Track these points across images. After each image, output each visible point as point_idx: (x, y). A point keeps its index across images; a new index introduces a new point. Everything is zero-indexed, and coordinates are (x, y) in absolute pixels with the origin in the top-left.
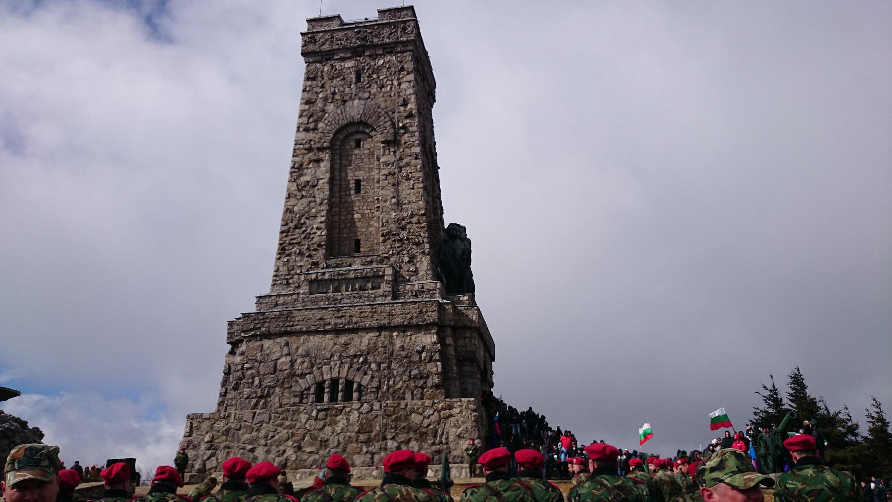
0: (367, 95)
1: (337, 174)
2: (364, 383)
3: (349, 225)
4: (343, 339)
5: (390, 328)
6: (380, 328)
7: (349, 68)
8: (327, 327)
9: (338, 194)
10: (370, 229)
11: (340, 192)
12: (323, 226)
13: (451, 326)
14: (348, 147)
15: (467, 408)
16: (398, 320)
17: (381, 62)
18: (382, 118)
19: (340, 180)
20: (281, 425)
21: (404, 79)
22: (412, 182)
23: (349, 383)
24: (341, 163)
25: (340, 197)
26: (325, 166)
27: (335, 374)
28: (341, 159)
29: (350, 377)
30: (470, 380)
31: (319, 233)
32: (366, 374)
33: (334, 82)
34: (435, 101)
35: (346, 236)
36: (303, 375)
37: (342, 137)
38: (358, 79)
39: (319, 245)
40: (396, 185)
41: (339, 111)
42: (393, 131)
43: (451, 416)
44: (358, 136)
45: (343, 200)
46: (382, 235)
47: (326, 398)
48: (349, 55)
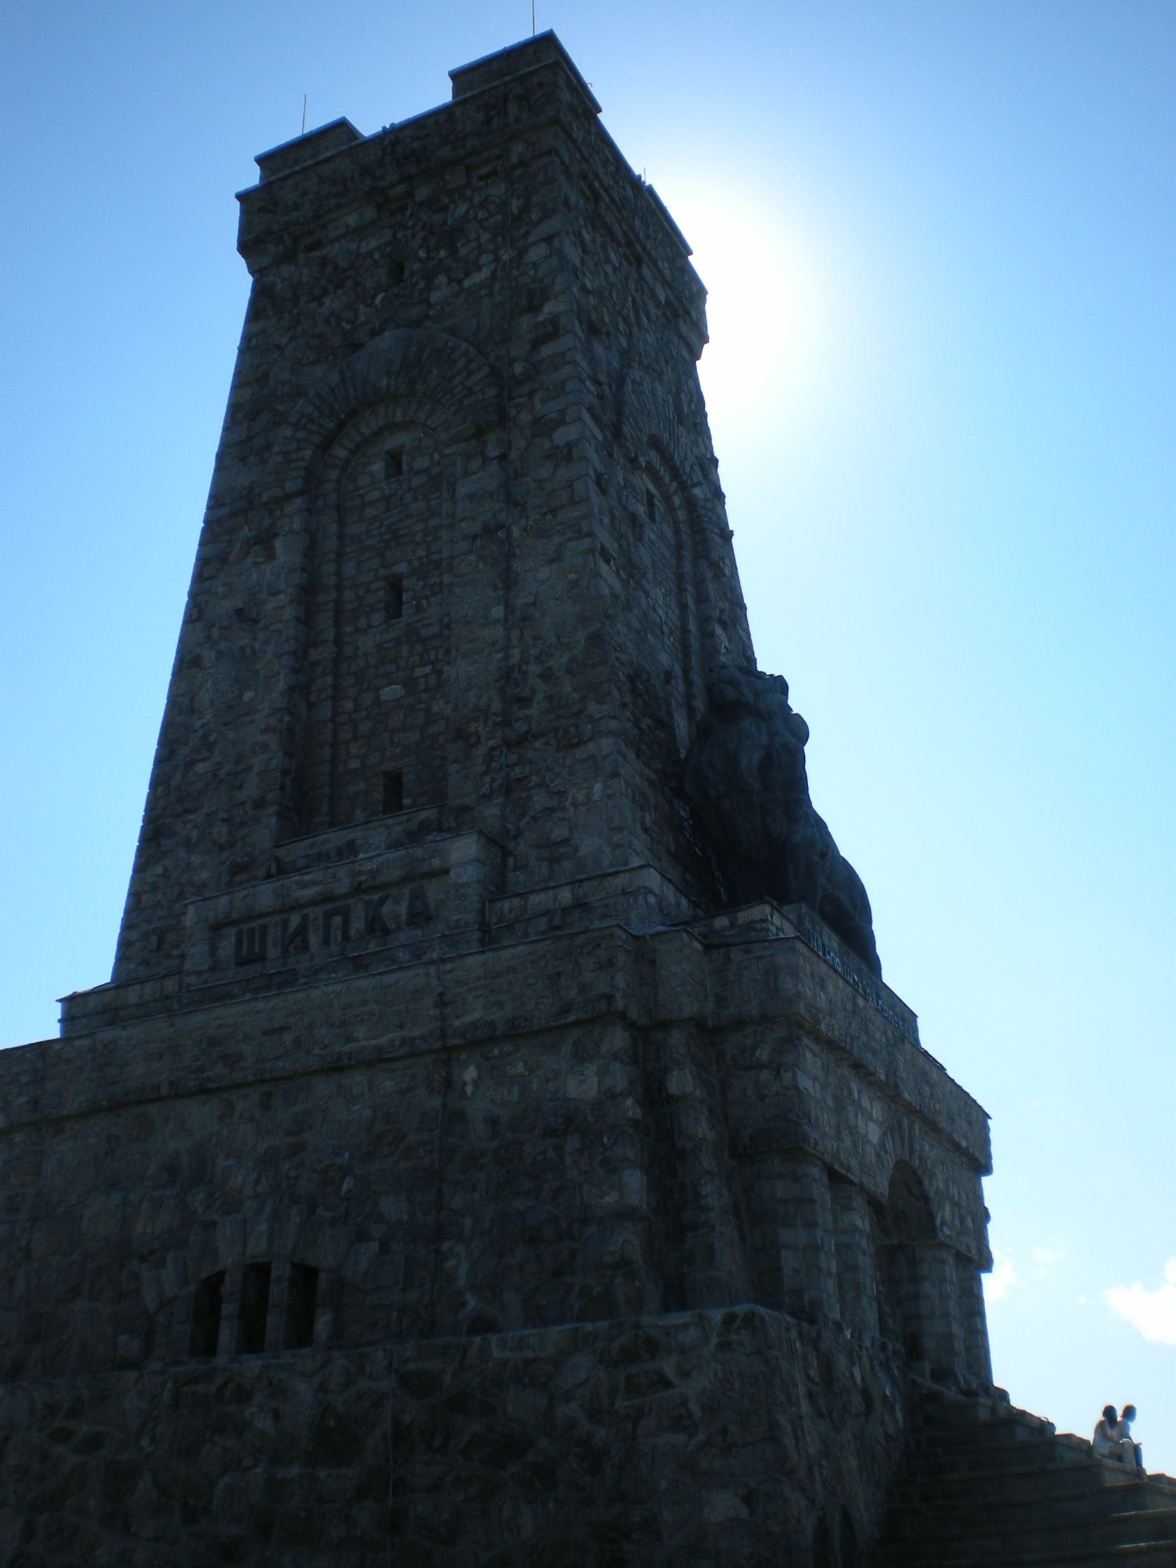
0: (416, 311)
1: (329, 568)
3: (365, 727)
7: (370, 253)
9: (330, 635)
10: (433, 729)
11: (337, 624)
12: (273, 740)
14: (364, 480)
17: (462, 208)
18: (461, 364)
19: (339, 588)
20: (64, 1436)
21: (532, 238)
22: (556, 539)
23: (305, 1275)
24: (341, 536)
25: (338, 641)
27: (257, 1247)
28: (341, 523)
32: (361, 1236)
33: (327, 301)
34: (704, 339)
35: (355, 764)
37: (342, 453)
38: (397, 271)
39: (259, 804)
41: (334, 378)
42: (491, 392)
44: (393, 442)
45: (348, 651)
47: (227, 1335)
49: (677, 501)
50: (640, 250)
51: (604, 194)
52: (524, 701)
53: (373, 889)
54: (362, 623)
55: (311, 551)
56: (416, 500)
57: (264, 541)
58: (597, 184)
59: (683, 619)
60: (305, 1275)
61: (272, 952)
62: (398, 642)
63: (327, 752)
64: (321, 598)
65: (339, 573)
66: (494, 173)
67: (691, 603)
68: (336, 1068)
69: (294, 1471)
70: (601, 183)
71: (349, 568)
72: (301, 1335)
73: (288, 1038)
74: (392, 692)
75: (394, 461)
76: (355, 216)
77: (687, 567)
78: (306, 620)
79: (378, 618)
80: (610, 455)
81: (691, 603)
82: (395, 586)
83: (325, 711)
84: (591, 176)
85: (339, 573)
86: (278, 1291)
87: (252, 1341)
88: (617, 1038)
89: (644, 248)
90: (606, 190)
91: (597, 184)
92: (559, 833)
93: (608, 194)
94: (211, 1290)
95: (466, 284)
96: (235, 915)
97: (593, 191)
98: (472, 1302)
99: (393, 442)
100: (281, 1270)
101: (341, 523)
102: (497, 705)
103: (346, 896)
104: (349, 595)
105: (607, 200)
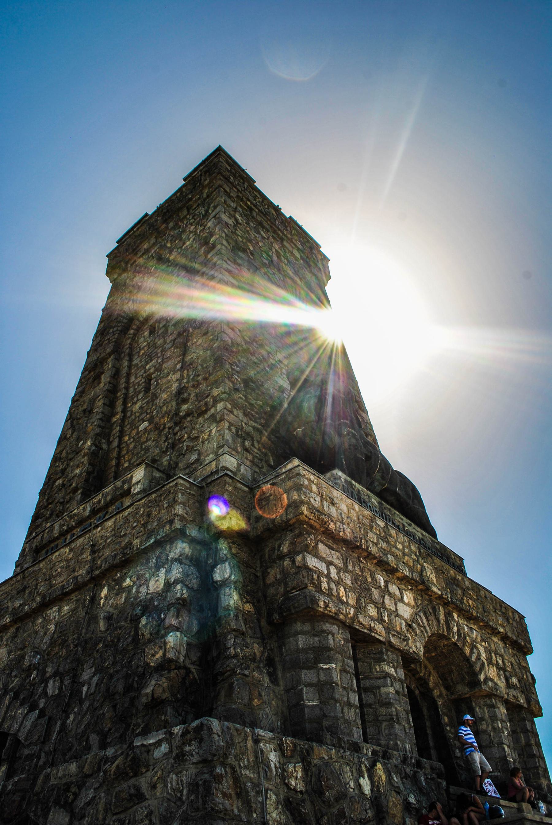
3: (131, 446)
11: (125, 403)
19: (127, 388)
24: (130, 367)
25: (124, 411)
30: (307, 676)
32: (32, 709)
45: (129, 414)
50: (281, 234)
51: (255, 208)
53: (100, 510)
54: (135, 399)
55: (116, 374)
56: (159, 339)
57: (98, 378)
58: (249, 203)
62: (148, 402)
63: (114, 462)
64: (119, 394)
65: (127, 382)
66: (199, 205)
70: (251, 203)
71: (133, 379)
76: (147, 244)
78: (111, 404)
83: (115, 444)
84: (244, 199)
85: (127, 382)
89: (283, 233)
90: (254, 206)
91: (249, 203)
92: (194, 457)
93: (256, 208)
95: (183, 248)
96: (44, 542)
97: (248, 207)
101: (131, 360)
103: (89, 517)
104: (131, 390)
105: (257, 210)
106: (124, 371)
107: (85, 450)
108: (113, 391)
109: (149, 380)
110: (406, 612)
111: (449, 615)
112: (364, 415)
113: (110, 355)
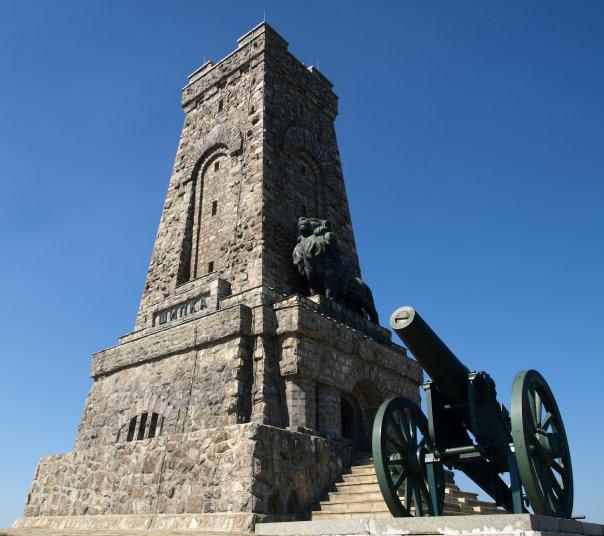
1: (197, 202)
2: (166, 415)
4: (159, 366)
5: (198, 348)
6: (188, 350)
8: (146, 357)
12: (178, 256)
13: (260, 335)
15: (243, 436)
16: (204, 336)
26: (187, 197)
29: (156, 411)
31: (174, 263)
36: (122, 412)
39: (172, 276)
40: (238, 194)
43: (227, 447)
45: (202, 226)
46: (222, 249)
48: (215, 89)
49: (315, 167)
52: (240, 237)
55: (193, 199)
57: (181, 195)
59: (316, 206)
60: (155, 416)
61: (168, 320)
67: (320, 200)
68: (170, 354)
69: (139, 475)
72: (152, 435)
73: (159, 345)
74: (212, 238)
75: (217, 165)
77: (319, 188)
79: (210, 215)
80: (278, 155)
81: (320, 200)
82: (215, 204)
85: (201, 203)
86: (149, 421)
87: (130, 439)
88: (238, 341)
94: (134, 421)
98: (193, 423)
99: (216, 161)
100: (150, 415)
102: (233, 238)
106: (198, 195)
107: (176, 250)
108: (191, 210)
109: (215, 204)
110: (345, 369)
111: (371, 369)
112: (349, 226)
113: (188, 181)
